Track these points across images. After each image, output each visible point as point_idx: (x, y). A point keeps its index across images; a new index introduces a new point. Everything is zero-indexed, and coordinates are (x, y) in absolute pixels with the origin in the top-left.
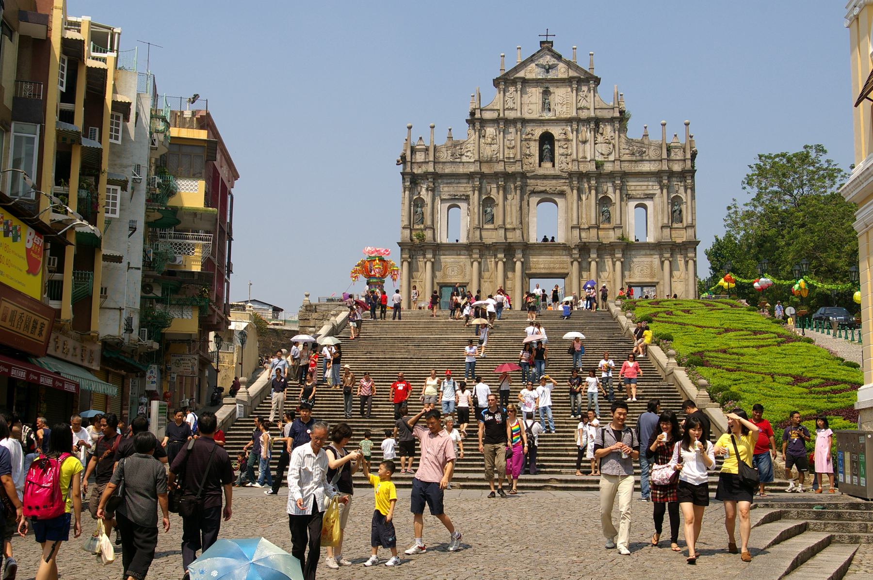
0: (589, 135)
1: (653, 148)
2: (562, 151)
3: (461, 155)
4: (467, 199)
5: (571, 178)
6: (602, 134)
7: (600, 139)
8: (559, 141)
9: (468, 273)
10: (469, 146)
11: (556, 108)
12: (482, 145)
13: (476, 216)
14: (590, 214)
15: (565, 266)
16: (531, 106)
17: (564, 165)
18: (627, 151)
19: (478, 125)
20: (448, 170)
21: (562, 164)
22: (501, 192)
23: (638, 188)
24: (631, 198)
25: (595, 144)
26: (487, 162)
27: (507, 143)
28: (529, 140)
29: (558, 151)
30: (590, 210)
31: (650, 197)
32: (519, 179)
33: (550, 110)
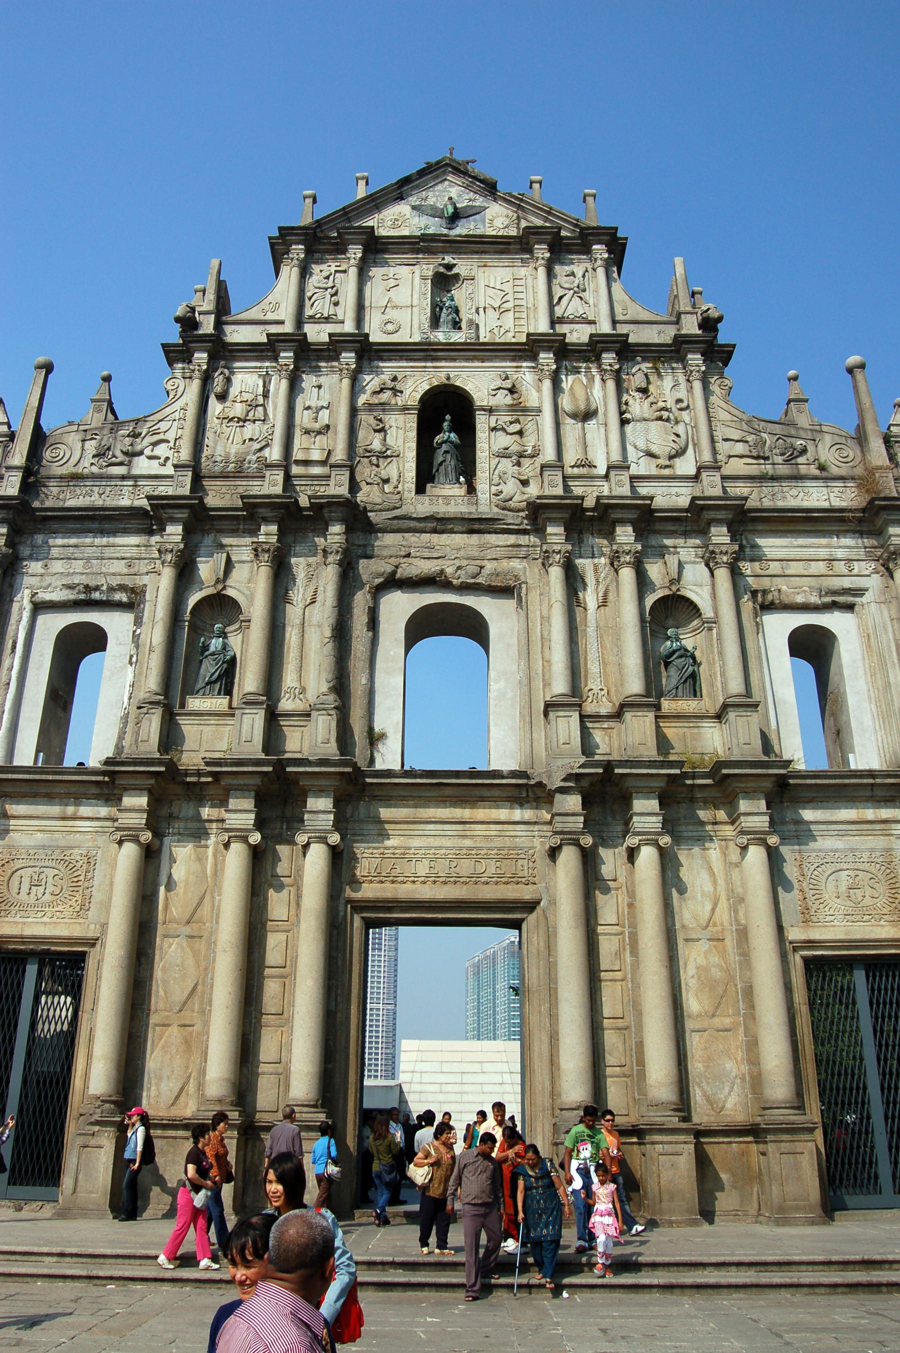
0: (601, 393)
1: (828, 439)
2: (502, 441)
3: (132, 454)
4: (132, 602)
5: (538, 530)
6: (644, 391)
7: (637, 406)
8: (490, 411)
9: (98, 896)
10: (163, 426)
11: (480, 320)
12: (212, 422)
13: (155, 663)
14: (618, 662)
15: (523, 868)
16: (391, 314)
17: (510, 488)
18: (740, 448)
19: (201, 357)
20: (77, 499)
21: (499, 480)
22: (264, 573)
23: (795, 568)
24: (769, 607)
25: (624, 422)
26: (224, 476)
27: (303, 418)
28: (384, 407)
29: (487, 442)
30: (618, 638)
31: (843, 601)
32: (336, 529)
33: (456, 325)
